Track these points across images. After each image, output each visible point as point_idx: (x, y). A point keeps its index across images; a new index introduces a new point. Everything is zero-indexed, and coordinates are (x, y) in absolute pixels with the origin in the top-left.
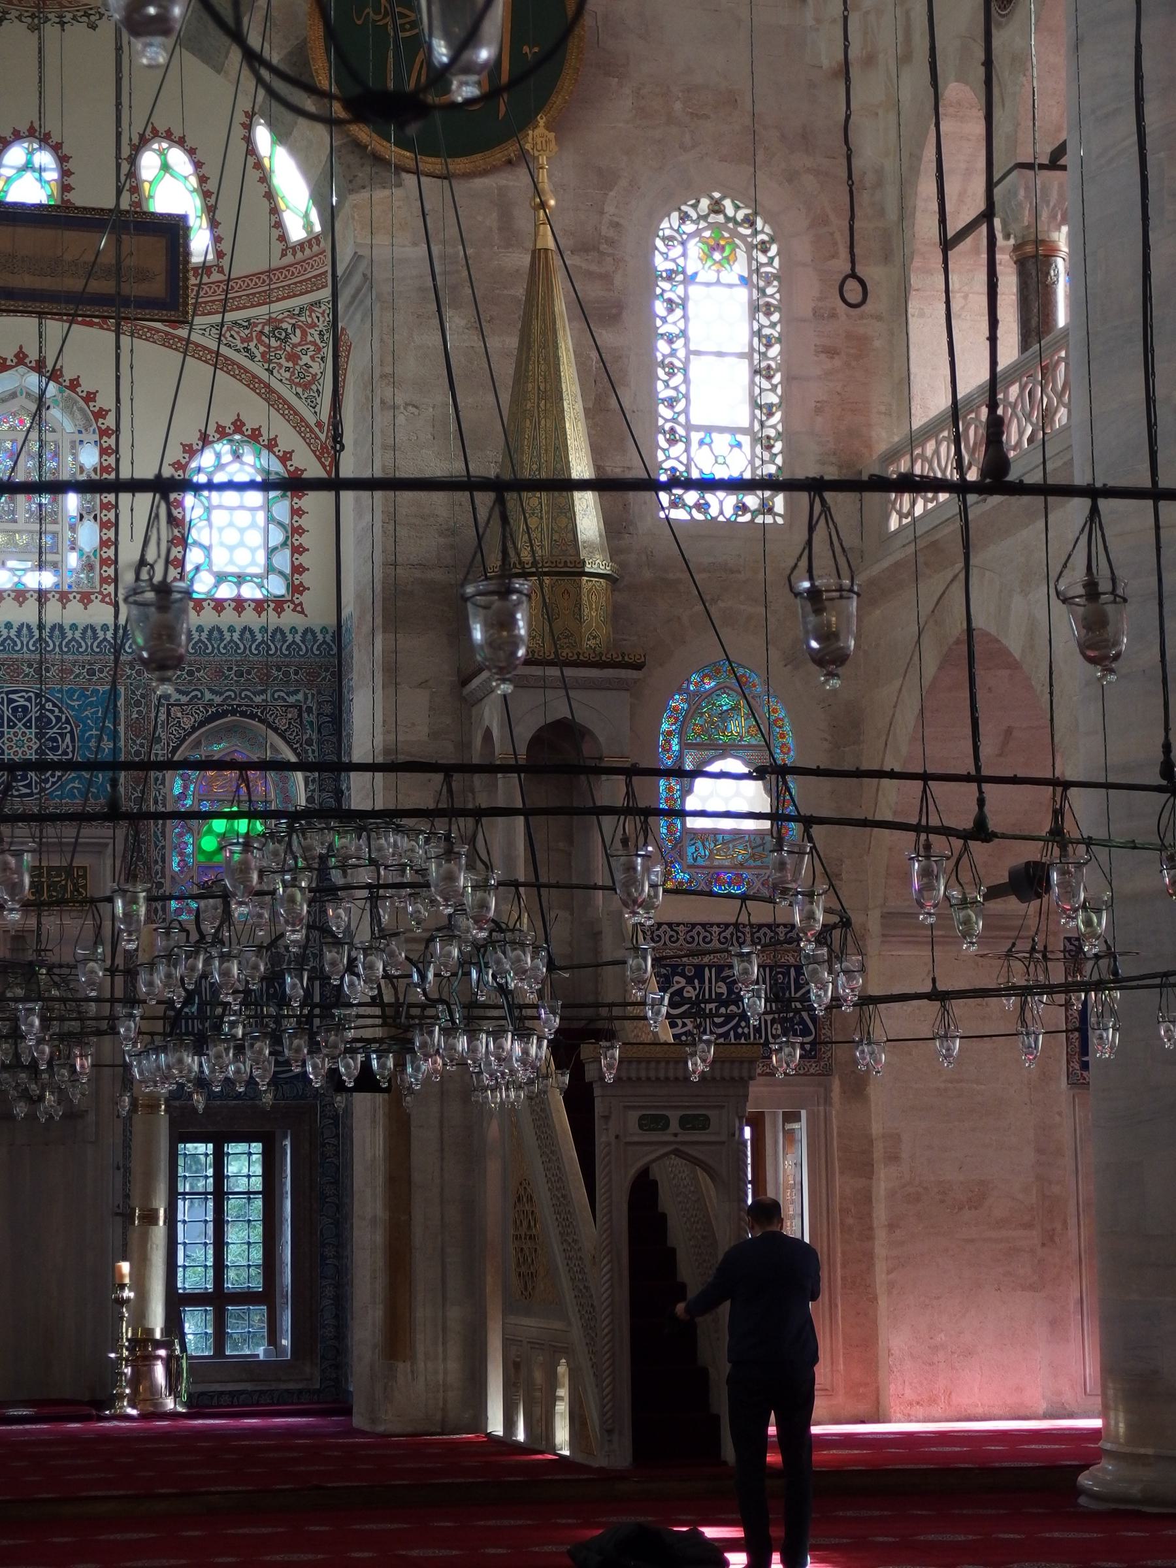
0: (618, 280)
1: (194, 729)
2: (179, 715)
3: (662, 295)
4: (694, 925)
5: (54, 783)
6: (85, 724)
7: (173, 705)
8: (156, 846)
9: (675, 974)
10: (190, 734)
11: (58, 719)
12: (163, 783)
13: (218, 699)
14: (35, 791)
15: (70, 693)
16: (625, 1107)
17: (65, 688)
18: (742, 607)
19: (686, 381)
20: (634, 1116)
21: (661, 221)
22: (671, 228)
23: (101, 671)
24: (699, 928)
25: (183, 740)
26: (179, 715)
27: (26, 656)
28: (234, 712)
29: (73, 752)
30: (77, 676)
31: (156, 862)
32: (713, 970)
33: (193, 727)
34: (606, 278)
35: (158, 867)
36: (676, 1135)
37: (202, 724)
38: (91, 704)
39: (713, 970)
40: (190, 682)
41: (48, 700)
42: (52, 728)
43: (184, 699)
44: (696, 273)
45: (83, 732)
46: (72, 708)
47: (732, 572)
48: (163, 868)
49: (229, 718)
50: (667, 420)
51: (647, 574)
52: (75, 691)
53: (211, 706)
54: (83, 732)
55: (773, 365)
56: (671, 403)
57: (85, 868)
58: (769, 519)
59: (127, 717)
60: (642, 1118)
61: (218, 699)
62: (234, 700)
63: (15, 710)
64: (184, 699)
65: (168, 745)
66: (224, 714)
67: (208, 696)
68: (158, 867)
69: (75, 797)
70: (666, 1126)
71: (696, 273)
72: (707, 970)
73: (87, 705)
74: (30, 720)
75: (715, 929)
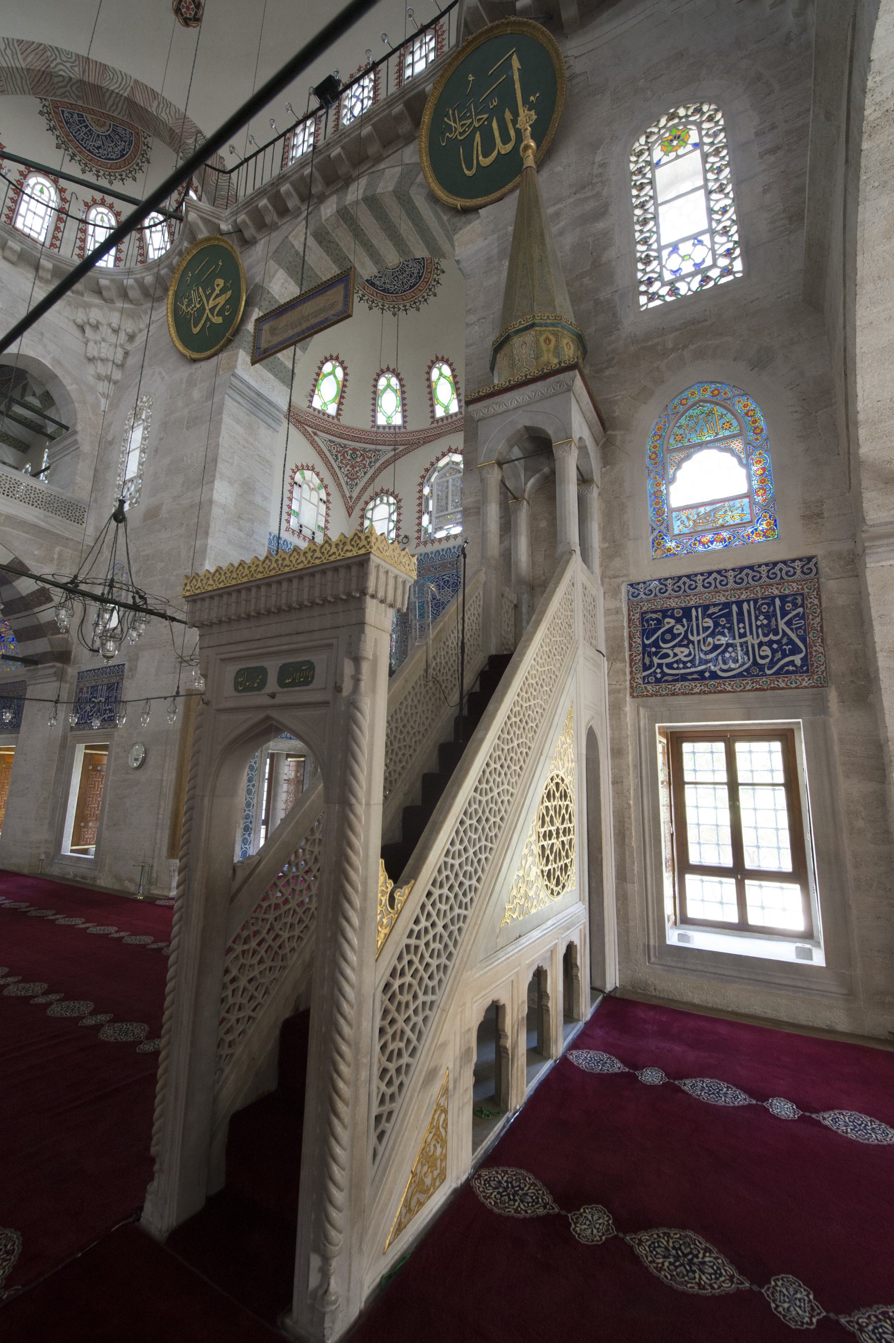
0: (605, 193)
3: (635, 184)
4: (680, 578)
9: (664, 617)
16: (222, 660)
18: (710, 342)
19: (657, 224)
20: (231, 670)
21: (634, 144)
22: (641, 145)
24: (684, 579)
32: (700, 610)
34: (598, 195)
36: (273, 696)
39: (700, 610)
44: (660, 160)
47: (699, 322)
50: (642, 252)
51: (632, 349)
55: (725, 182)
56: (645, 241)
58: (731, 278)
60: (239, 673)
70: (263, 684)
71: (660, 160)
72: (693, 610)
75: (699, 577)
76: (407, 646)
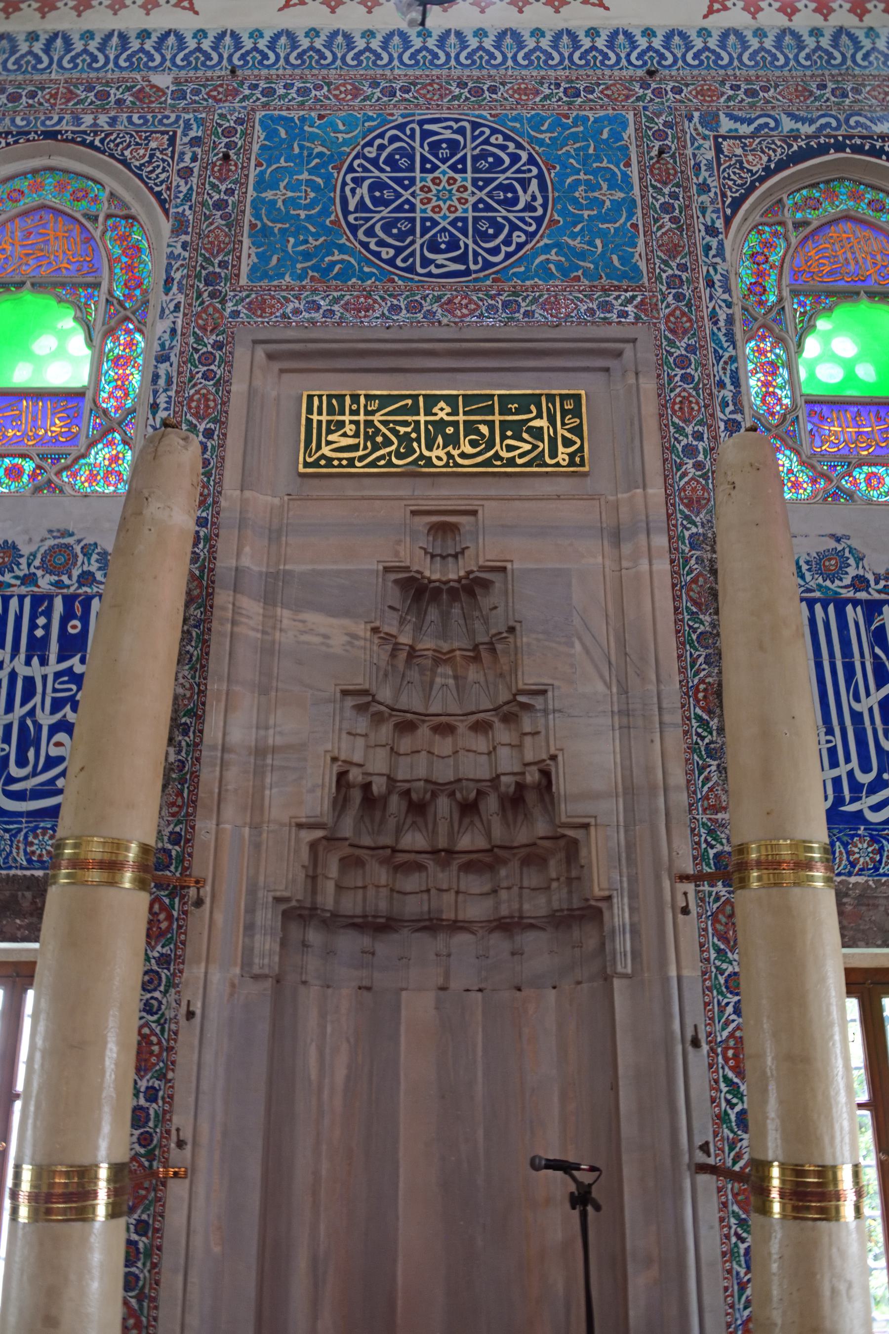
1: (769, 173)
2: (739, 151)
5: (508, 255)
6: (564, 166)
7: (725, 138)
8: (719, 358)
10: (762, 180)
11: (515, 158)
12: (721, 253)
13: (807, 129)
14: (473, 267)
15: (536, 123)
17: (526, 114)
23: (589, 90)
25: (752, 189)
26: (739, 151)
27: (457, 72)
28: (840, 147)
29: (545, 206)
30: (546, 97)
31: (721, 385)
33: (767, 169)
35: (727, 393)
37: (782, 165)
38: (575, 137)
40: (752, 106)
41: (494, 131)
42: (504, 171)
43: (745, 129)
45: (562, 177)
46: (541, 143)
48: (737, 395)
49: (833, 156)
52: (543, 120)
53: (796, 138)
54: (562, 177)
57: (577, 398)
59: (641, 155)
61: (807, 129)
62: (836, 129)
63: (435, 147)
64: (745, 129)
65: (724, 195)
66: (823, 150)
67: (788, 124)
68: (727, 393)
69: (551, 276)
73: (567, 138)
74: (463, 160)
76: (223, 384)
